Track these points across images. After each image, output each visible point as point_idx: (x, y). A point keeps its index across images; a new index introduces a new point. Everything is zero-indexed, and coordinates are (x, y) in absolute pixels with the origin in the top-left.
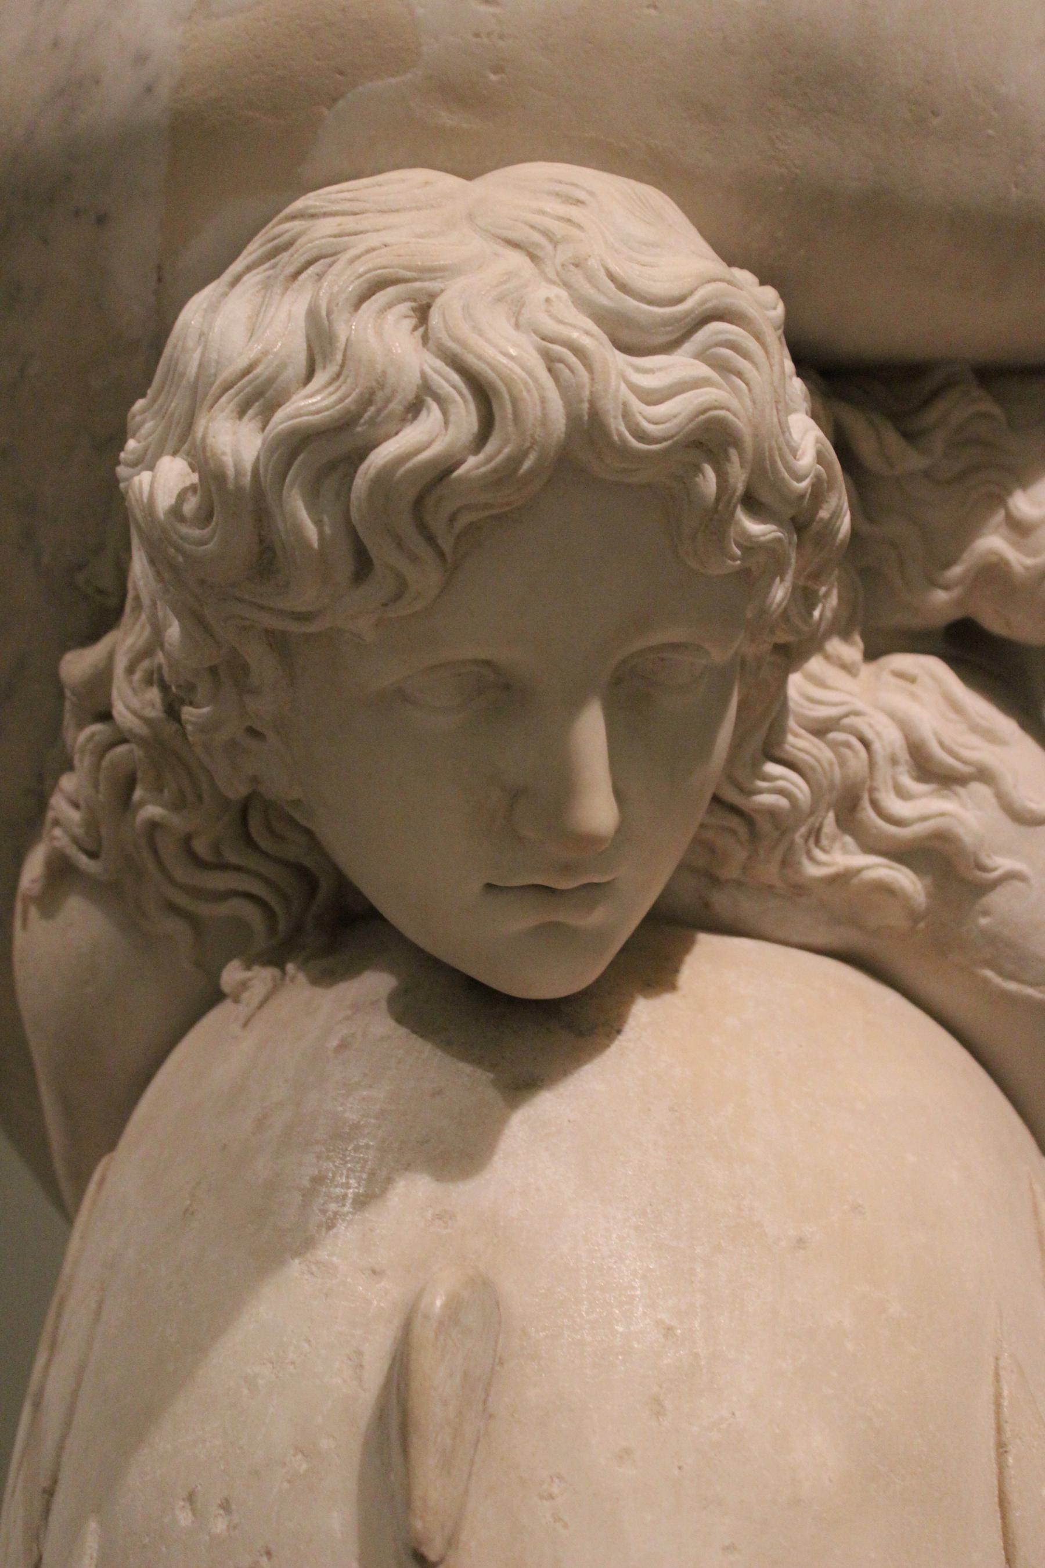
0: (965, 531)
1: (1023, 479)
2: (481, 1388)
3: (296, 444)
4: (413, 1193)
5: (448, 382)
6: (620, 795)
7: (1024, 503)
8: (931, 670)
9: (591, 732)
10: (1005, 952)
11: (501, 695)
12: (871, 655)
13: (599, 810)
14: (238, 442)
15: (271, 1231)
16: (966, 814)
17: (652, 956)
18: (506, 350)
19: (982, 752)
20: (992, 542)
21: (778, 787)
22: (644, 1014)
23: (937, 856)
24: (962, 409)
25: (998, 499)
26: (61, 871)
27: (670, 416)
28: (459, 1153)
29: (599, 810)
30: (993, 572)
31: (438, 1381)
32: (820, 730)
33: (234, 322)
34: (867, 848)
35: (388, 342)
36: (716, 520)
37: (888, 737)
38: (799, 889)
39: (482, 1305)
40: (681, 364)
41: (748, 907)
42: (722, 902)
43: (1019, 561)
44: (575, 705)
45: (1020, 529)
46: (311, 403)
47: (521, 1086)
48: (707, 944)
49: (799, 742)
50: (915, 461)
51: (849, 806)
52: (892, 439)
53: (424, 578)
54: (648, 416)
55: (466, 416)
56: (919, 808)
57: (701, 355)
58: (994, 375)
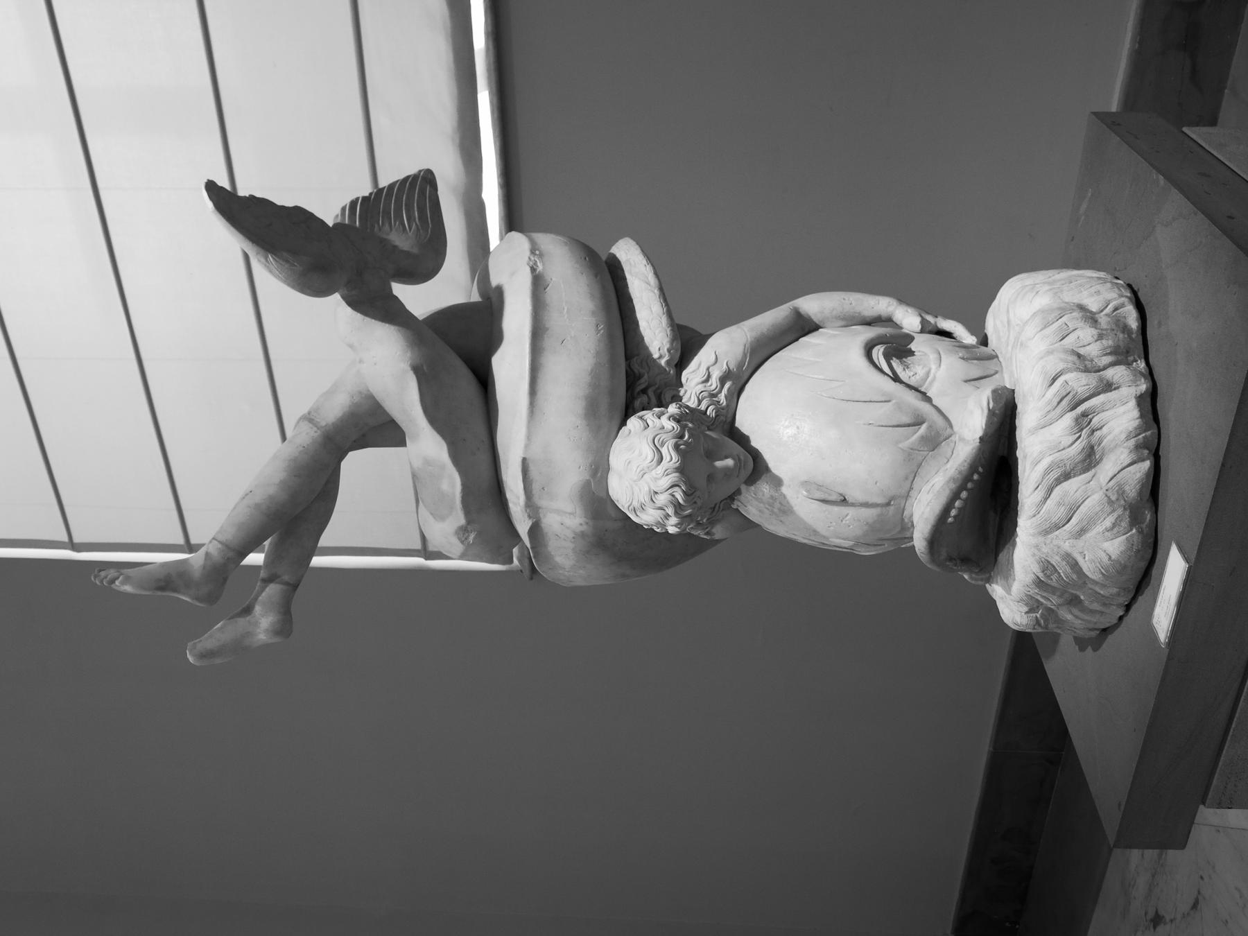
0: (660, 366)
1: (650, 355)
2: (819, 487)
3: (676, 513)
4: (784, 490)
5: (670, 491)
6: (726, 457)
7: (656, 356)
8: (685, 374)
9: (719, 464)
10: (740, 365)
11: (710, 478)
12: (682, 386)
13: (729, 462)
14: (674, 520)
15: (785, 510)
16: (716, 374)
17: (742, 440)
18: (666, 482)
19: (703, 370)
20: (663, 362)
21: (711, 412)
22: (754, 443)
23: (723, 380)
24: (636, 368)
25: (654, 360)
26: (707, 534)
27: (675, 457)
28: (778, 482)
29: (729, 462)
30: (668, 362)
31: (819, 495)
32: (700, 402)
33: (647, 518)
34: (720, 391)
35: (663, 499)
36: (686, 443)
37: (701, 387)
38: (728, 405)
39: (805, 484)
40: (664, 451)
41: (730, 415)
42: (729, 420)
43: (666, 358)
44: (714, 467)
45: (661, 357)
46: (670, 511)
47: (767, 469)
48: (737, 424)
49: (703, 407)
50: (646, 377)
51: (713, 395)
52: (642, 380)
53: (698, 493)
54: (675, 459)
55: (676, 489)
56: (714, 382)
57: (662, 445)
58: (628, 358)
